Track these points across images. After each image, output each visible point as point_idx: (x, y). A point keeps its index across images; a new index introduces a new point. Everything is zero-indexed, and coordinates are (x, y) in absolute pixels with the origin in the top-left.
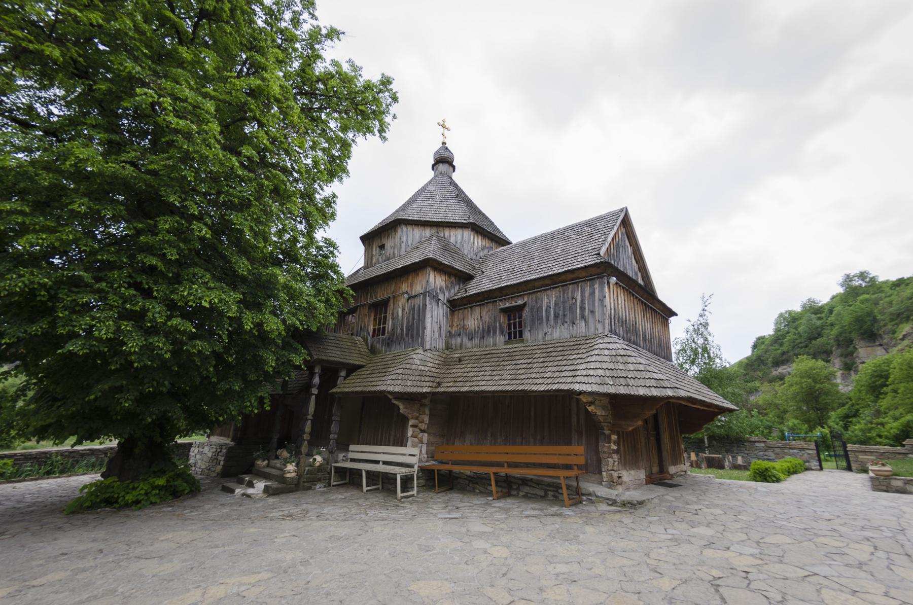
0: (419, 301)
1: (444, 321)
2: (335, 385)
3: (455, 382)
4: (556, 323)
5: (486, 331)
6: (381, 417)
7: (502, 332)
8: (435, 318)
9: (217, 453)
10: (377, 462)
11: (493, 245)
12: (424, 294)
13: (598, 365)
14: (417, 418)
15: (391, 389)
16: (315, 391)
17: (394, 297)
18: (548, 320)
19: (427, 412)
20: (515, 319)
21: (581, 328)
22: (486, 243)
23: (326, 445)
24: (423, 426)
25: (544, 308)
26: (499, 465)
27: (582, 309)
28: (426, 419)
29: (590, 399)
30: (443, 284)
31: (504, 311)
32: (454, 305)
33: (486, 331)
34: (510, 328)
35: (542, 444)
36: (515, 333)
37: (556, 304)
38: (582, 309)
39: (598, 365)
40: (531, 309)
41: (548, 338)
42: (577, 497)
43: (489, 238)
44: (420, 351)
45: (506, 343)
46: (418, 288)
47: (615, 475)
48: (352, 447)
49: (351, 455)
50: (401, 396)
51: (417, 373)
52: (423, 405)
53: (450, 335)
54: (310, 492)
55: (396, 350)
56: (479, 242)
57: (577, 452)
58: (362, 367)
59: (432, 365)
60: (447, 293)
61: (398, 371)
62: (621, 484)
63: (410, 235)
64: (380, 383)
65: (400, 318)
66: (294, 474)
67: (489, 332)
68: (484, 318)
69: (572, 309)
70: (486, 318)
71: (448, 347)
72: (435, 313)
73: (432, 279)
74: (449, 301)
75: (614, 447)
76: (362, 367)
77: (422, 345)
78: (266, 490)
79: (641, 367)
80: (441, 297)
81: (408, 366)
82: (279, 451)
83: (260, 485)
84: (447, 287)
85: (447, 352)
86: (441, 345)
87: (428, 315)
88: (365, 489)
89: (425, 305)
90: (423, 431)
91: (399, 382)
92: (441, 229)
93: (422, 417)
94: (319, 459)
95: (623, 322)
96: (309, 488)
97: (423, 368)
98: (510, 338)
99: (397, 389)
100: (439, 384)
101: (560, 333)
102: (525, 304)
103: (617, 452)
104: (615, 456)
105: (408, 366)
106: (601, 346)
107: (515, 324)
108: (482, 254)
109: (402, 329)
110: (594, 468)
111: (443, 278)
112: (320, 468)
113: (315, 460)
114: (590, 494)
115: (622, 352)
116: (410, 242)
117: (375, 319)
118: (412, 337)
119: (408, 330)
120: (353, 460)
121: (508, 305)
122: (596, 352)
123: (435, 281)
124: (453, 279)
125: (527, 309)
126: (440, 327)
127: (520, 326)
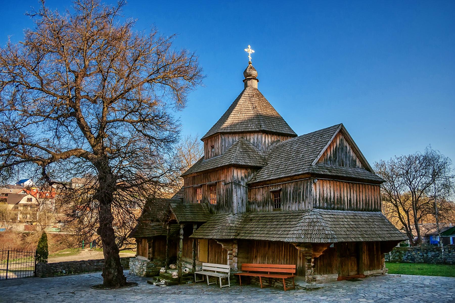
2: (191, 233)
3: (245, 233)
4: (293, 201)
5: (265, 203)
8: (238, 195)
10: (214, 271)
11: (280, 138)
12: (232, 183)
13: (300, 228)
14: (232, 250)
15: (215, 237)
16: (182, 237)
17: (219, 182)
18: (290, 200)
19: (237, 247)
20: (277, 197)
21: (302, 206)
22: (274, 138)
24: (234, 254)
25: (289, 193)
27: (303, 195)
28: (236, 251)
30: (243, 175)
31: (271, 192)
32: (250, 187)
34: (275, 202)
35: (287, 264)
36: (277, 205)
37: (293, 192)
38: (303, 195)
39: (300, 228)
40: (283, 193)
41: (290, 209)
42: (295, 288)
43: (276, 135)
44: (231, 215)
45: (274, 210)
46: (229, 180)
47: (311, 277)
48: (203, 264)
49: (204, 268)
50: (220, 240)
51: (229, 228)
52: (234, 243)
53: (249, 203)
54: (185, 285)
55: (222, 213)
56: (268, 139)
57: (291, 268)
58: (205, 222)
59: (237, 222)
60: (246, 180)
61: (219, 228)
62: (315, 281)
63: (227, 141)
64: (210, 234)
65: (222, 195)
66: (177, 277)
67: (266, 204)
68: (264, 195)
69: (299, 195)
70: (265, 195)
71: (248, 210)
72: (239, 193)
73: (235, 174)
74: (247, 184)
75: (312, 264)
76: (205, 222)
77: (232, 212)
78: (166, 283)
79: (321, 228)
80: (242, 184)
81: (224, 224)
82: (170, 266)
83: (163, 281)
84: (245, 176)
86: (244, 210)
87: (234, 195)
88: (208, 284)
89: (232, 190)
90: (235, 256)
91: (219, 233)
92: (244, 135)
95: (326, 200)
96: (185, 283)
98: (275, 208)
99: (218, 237)
100: (239, 234)
101: (294, 207)
102: (280, 190)
104: (312, 268)
105: (224, 224)
106: (306, 217)
107: (277, 199)
108: (271, 147)
109: (223, 201)
111: (243, 171)
112: (190, 274)
113: (186, 270)
114: (298, 286)
115: (315, 220)
116: (227, 145)
118: (228, 206)
119: (226, 202)
120: (205, 270)
121: (274, 189)
122: (302, 221)
123: (238, 174)
124: (249, 170)
125: (281, 193)
126: (242, 201)
127: (279, 202)
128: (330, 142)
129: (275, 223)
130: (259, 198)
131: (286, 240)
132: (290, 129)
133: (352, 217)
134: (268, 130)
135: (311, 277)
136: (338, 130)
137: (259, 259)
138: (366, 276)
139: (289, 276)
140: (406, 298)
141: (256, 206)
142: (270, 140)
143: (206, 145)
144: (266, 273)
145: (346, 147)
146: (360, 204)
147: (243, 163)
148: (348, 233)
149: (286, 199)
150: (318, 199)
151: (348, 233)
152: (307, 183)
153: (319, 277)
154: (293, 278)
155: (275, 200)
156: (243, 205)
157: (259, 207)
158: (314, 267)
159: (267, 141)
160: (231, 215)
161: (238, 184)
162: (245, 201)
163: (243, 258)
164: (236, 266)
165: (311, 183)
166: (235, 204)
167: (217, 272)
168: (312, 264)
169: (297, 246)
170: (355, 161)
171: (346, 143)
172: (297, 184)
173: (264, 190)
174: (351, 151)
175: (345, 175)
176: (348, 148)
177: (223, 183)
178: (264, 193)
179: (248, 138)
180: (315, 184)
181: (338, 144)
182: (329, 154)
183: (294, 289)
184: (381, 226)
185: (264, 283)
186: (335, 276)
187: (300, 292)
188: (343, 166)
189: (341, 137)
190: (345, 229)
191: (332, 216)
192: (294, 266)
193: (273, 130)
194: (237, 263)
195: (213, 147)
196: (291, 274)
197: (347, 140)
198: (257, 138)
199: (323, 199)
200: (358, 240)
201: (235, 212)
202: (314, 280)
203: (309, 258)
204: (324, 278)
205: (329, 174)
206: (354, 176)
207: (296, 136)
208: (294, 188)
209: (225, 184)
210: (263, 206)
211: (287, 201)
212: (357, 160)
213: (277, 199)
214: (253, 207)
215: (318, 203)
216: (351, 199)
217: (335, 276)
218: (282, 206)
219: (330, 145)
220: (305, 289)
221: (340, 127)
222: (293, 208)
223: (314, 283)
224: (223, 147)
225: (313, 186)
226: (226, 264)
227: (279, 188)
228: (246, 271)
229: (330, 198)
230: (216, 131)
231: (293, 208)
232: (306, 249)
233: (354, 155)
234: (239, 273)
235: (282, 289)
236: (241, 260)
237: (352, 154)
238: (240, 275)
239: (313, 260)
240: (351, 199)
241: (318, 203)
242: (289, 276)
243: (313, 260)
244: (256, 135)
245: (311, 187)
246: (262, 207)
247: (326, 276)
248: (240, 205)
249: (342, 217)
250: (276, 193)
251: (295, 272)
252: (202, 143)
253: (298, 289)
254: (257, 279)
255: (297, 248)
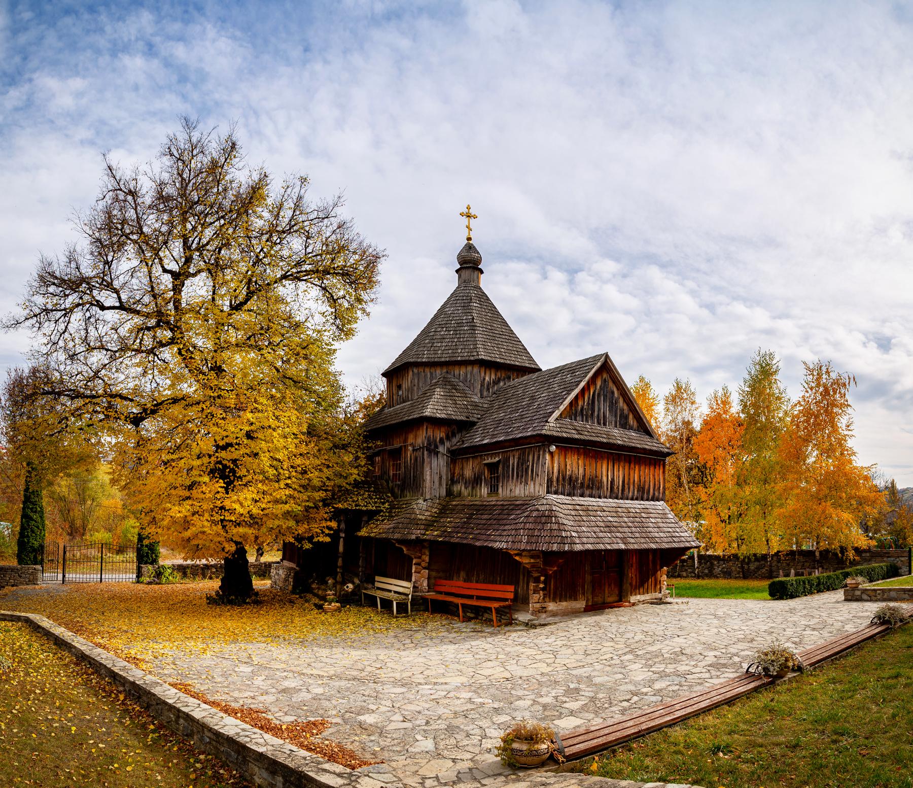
0: (419, 453)
1: (444, 471)
6: (392, 558)
7: (486, 484)
9: (287, 576)
10: (390, 591)
14: (420, 558)
23: (357, 575)
24: (423, 564)
26: (470, 597)
28: (427, 559)
29: (516, 552)
30: (443, 435)
31: (486, 464)
32: (456, 456)
33: (476, 481)
41: (513, 495)
42: (510, 622)
44: (421, 501)
48: (377, 578)
49: (377, 585)
52: (424, 547)
71: (449, 493)
74: (449, 451)
79: (555, 527)
85: (447, 499)
86: (443, 492)
90: (425, 568)
92: (450, 368)
93: (424, 557)
94: (351, 586)
97: (421, 517)
102: (499, 461)
103: (543, 589)
110: (520, 601)
111: (443, 429)
117: (393, 465)
120: (379, 588)
121: (490, 461)
125: (501, 466)
126: (441, 478)
128: (582, 384)
129: (485, 517)
130: (468, 473)
131: (497, 545)
132: (531, 359)
133: (611, 509)
134: (489, 359)
135: (538, 605)
136: (599, 364)
137: (463, 574)
138: (634, 604)
139: (502, 604)
140: (677, 639)
141: (463, 488)
142: (493, 377)
143: (389, 383)
144: (470, 597)
145: (613, 393)
146: (629, 488)
147: (443, 416)
148: (601, 535)
149: (506, 477)
150: (555, 479)
151: (601, 535)
152: (539, 451)
153: (552, 606)
154: (509, 607)
155: (491, 478)
156: (440, 484)
157: (466, 488)
158: (543, 589)
159: (487, 378)
160: (421, 501)
161: (434, 450)
162: (444, 477)
163: (437, 571)
164: (425, 584)
165: (544, 451)
166: (428, 483)
167: (395, 592)
168: (542, 586)
169: (517, 555)
170: (627, 417)
171: (611, 384)
172: (524, 453)
173: (476, 462)
174: (621, 400)
175: (605, 441)
176: (616, 395)
177: (410, 448)
178: (475, 464)
179: (457, 372)
180: (551, 454)
181: (598, 387)
182: (580, 403)
183: (511, 624)
184: (661, 525)
185: (468, 614)
186: (581, 604)
187: (516, 631)
188: (605, 424)
189: (605, 376)
190: (597, 529)
191: (578, 507)
192: (511, 588)
193: (498, 360)
194: (429, 579)
195: (399, 387)
196: (506, 600)
197: (614, 382)
198: (471, 373)
199: (564, 479)
200: (615, 547)
201: (428, 497)
202: (543, 610)
203: (536, 575)
204: (560, 607)
205: (577, 436)
206: (619, 442)
207: (540, 370)
208: (519, 458)
209: (413, 450)
210: (473, 488)
211: (508, 481)
212: (631, 416)
213: (495, 475)
214: (456, 488)
215: (555, 484)
216: (613, 480)
217: (581, 604)
218: (500, 490)
219: (583, 390)
220: (527, 624)
221: (603, 359)
222: (517, 492)
223: (544, 616)
224: (415, 388)
225: (548, 457)
226: (410, 581)
227: (497, 459)
228: (441, 593)
229: (577, 479)
230: (405, 360)
231: (517, 492)
232: (532, 561)
233: (625, 407)
234: (431, 595)
235: (489, 622)
236: (434, 574)
237: (621, 403)
238: (430, 597)
239: (542, 578)
240: (613, 480)
241: (555, 484)
242: (502, 604)
243: (542, 578)
244: (469, 368)
245: (544, 458)
246: (470, 488)
247: (564, 604)
248: (437, 483)
249: (596, 508)
250: (493, 467)
251: (511, 596)
252: (384, 379)
253: (517, 624)
254: (457, 606)
255: (517, 558)
